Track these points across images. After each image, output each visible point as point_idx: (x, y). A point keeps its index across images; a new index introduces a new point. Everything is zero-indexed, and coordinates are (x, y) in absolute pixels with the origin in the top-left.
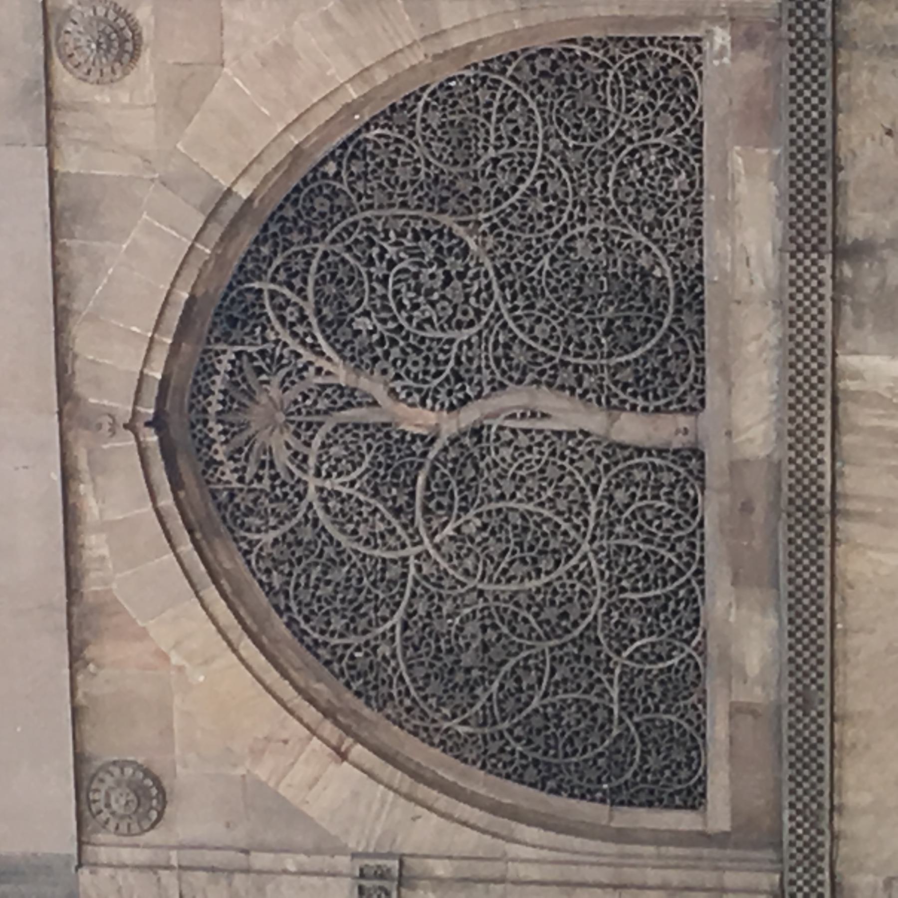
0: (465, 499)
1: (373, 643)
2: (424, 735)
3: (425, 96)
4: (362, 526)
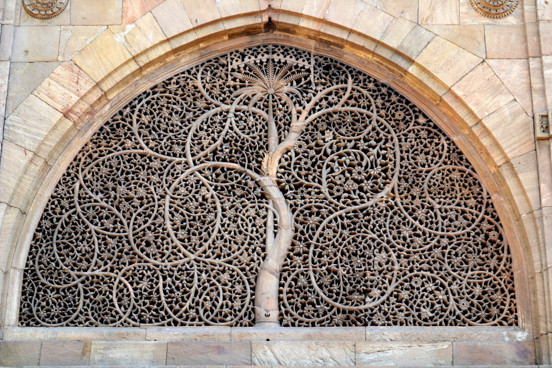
0: (222, 189)
1: (133, 137)
2: (75, 164)
3: (468, 171)
4: (206, 133)
